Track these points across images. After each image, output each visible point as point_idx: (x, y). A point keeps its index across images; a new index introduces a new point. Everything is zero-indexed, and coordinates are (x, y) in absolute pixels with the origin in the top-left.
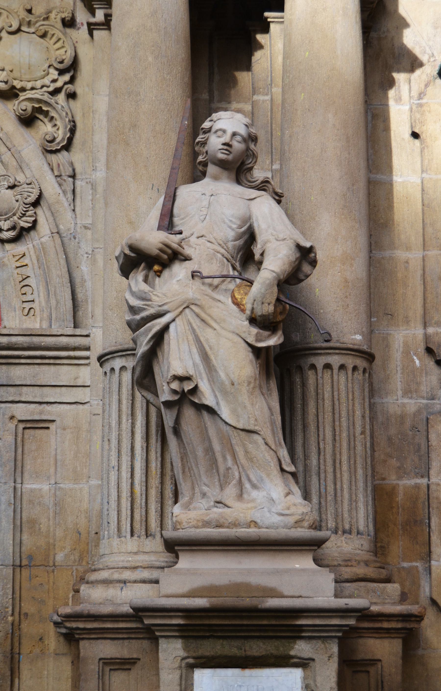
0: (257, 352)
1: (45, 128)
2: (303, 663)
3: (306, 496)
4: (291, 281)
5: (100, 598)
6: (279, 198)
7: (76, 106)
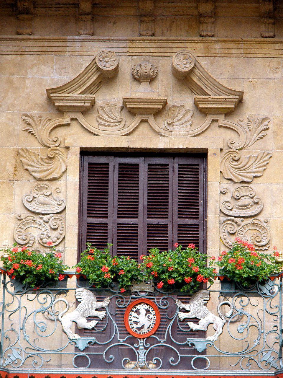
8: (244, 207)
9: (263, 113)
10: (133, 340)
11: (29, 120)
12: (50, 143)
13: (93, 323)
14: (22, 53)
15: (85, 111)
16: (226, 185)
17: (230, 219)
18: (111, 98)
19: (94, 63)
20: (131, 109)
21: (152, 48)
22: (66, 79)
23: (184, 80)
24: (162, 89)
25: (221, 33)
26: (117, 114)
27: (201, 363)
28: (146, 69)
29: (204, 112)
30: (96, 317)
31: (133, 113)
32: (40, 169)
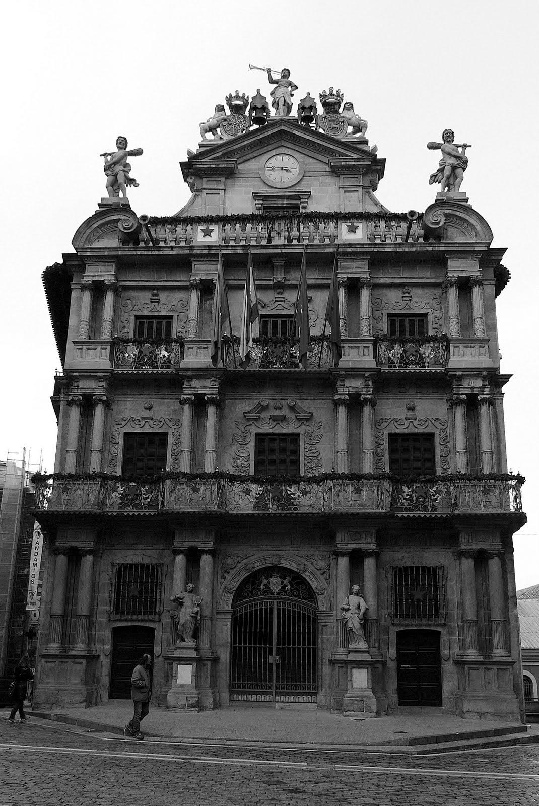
0: (360, 624)
2: (367, 668)
3: (368, 644)
4: (364, 613)
5: (338, 657)
6: (363, 598)
7: (330, 571)
8: (313, 453)
11: (237, 423)
12: (246, 432)
14: (235, 399)
15: (256, 420)
16: (307, 445)
17: (308, 458)
18: (265, 415)
19: (260, 403)
20: (274, 419)
21: (280, 397)
22: (250, 408)
23: (292, 408)
24: (285, 412)
27: (296, 509)
28: (278, 404)
29: (299, 420)
30: (259, 494)
31: (273, 420)
32: (241, 440)
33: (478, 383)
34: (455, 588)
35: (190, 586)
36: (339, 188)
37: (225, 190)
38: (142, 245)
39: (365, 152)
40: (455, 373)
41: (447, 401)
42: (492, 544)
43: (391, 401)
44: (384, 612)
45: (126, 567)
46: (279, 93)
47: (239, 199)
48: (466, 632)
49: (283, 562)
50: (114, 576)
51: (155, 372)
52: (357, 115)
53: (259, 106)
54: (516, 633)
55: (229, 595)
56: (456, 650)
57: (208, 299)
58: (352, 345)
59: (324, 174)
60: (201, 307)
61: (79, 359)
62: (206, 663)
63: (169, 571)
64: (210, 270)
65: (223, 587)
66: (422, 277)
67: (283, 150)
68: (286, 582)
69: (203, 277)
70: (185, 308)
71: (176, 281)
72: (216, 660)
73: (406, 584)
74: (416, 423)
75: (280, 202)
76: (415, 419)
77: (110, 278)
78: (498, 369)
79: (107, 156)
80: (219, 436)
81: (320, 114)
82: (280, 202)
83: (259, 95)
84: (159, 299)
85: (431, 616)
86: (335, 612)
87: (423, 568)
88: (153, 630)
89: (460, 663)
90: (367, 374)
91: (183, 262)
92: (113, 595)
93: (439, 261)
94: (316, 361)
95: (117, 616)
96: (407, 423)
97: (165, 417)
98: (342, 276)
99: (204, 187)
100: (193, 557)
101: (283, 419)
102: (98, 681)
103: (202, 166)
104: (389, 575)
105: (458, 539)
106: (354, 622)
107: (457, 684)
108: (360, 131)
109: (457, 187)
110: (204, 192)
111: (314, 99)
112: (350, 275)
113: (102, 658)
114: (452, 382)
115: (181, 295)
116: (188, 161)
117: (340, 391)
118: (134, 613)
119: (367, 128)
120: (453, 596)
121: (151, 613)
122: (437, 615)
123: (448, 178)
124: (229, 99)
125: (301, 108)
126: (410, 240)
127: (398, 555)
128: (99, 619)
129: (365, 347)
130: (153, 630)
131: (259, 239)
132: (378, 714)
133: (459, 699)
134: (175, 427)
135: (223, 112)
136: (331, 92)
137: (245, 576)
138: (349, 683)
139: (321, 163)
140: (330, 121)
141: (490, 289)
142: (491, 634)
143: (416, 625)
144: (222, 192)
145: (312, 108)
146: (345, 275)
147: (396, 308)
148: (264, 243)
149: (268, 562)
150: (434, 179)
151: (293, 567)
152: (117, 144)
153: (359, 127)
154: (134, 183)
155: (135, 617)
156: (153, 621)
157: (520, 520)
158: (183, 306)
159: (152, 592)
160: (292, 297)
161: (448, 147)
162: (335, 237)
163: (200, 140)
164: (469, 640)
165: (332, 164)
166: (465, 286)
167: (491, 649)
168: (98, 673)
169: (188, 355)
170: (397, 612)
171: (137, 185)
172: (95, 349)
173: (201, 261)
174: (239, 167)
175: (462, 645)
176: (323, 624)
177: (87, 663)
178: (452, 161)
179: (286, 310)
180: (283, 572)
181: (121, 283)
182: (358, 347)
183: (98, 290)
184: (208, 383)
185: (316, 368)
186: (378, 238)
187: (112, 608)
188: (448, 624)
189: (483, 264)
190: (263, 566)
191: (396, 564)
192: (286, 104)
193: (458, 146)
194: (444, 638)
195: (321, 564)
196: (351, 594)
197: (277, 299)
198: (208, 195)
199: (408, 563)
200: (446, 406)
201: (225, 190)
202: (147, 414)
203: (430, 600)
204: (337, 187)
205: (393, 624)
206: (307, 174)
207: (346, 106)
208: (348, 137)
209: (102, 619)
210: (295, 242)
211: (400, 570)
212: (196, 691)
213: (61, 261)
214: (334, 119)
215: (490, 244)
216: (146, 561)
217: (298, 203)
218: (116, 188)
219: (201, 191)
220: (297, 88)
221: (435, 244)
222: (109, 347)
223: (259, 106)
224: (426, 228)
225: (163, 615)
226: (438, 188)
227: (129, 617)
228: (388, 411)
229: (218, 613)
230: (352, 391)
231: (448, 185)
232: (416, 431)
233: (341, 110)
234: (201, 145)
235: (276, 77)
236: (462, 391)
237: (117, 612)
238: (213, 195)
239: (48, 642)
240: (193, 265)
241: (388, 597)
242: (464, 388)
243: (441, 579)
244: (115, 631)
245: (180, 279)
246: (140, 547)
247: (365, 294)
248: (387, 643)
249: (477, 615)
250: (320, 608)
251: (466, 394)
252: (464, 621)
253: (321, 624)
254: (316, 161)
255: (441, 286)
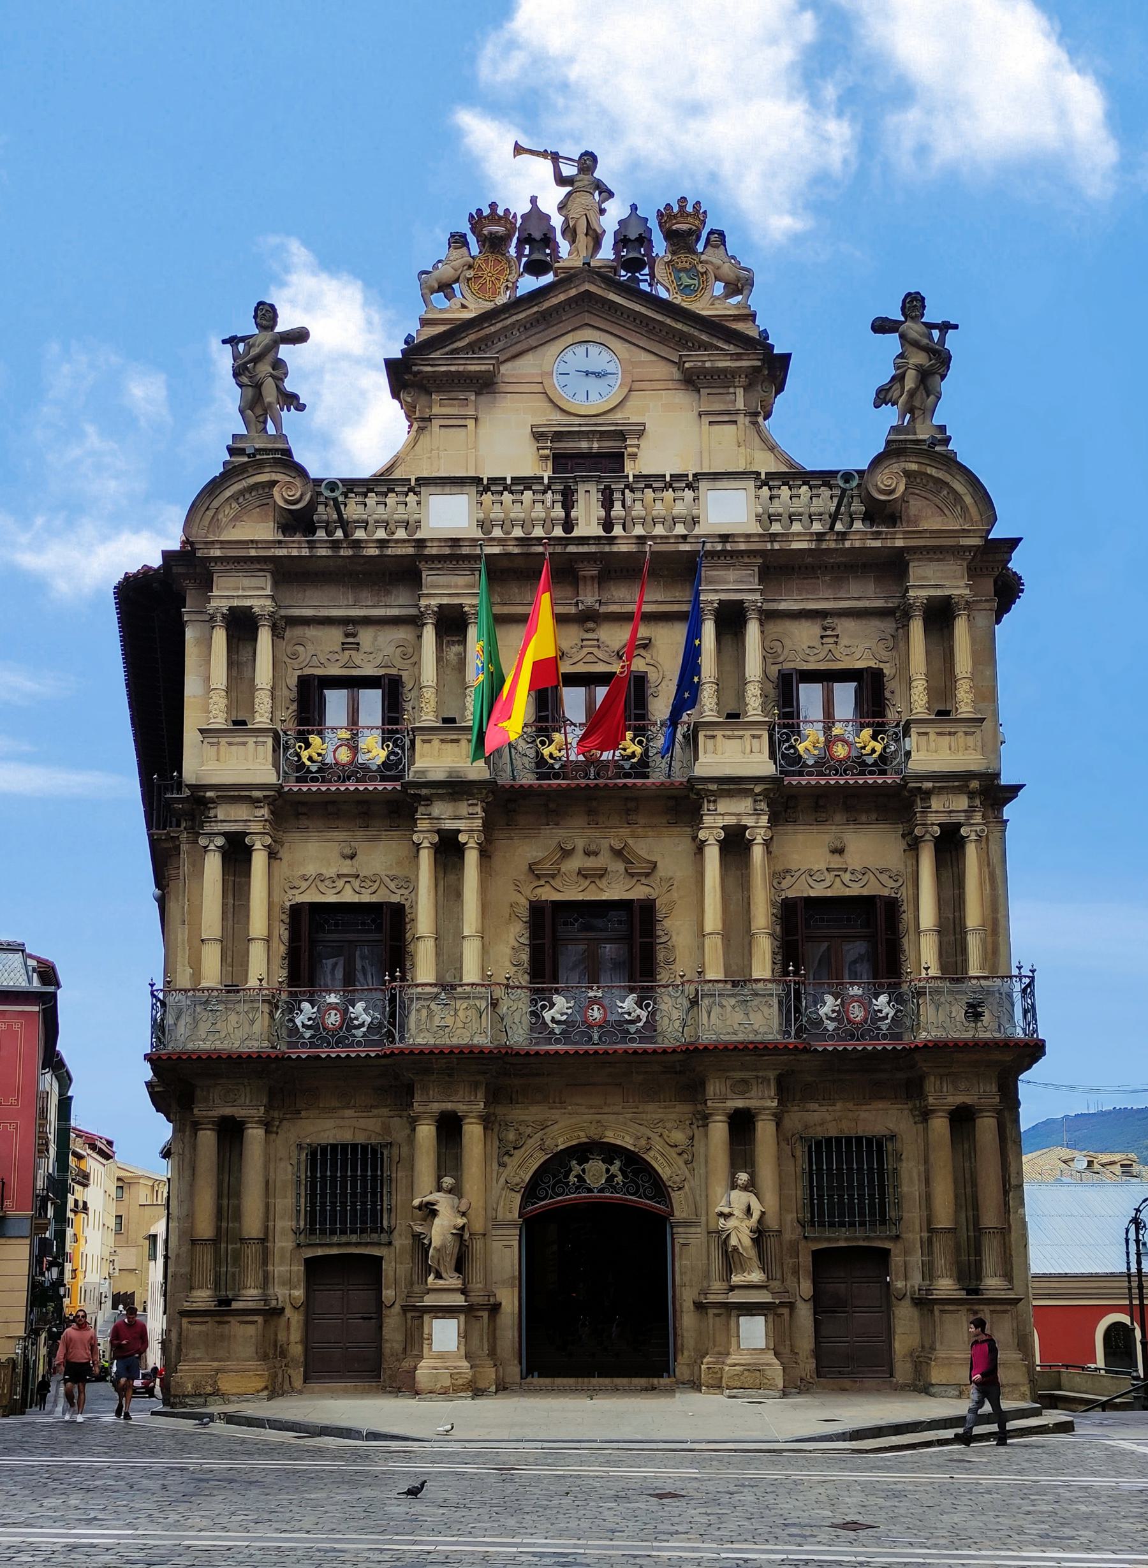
1: (685, 1156)
9: (670, 874)
10: (590, 1026)
13: (565, 1017)
14: (511, 838)
15: (553, 876)
20: (582, 874)
22: (541, 855)
23: (618, 854)
24: (604, 860)
25: (642, 821)
26: (575, 878)
28: (593, 847)
29: (632, 875)
31: (585, 877)
33: (962, 802)
34: (915, 1175)
35: (448, 1181)
36: (700, 415)
37: (476, 419)
38: (321, 534)
39: (747, 342)
40: (919, 785)
41: (903, 836)
42: (979, 1093)
43: (800, 837)
44: (790, 1217)
45: (324, 1149)
46: (576, 209)
47: (504, 439)
48: (936, 1249)
49: (609, 1133)
50: (303, 1168)
51: (361, 788)
52: (733, 257)
53: (537, 235)
54: (1021, 1249)
55: (514, 1194)
56: (916, 1280)
57: (454, 643)
58: (729, 733)
59: (670, 385)
60: (439, 660)
61: (212, 765)
62: (480, 1313)
63: (403, 1155)
64: (456, 587)
65: (502, 1180)
66: (859, 599)
67: (588, 334)
68: (615, 1168)
69: (445, 601)
70: (408, 661)
71: (386, 606)
72: (495, 1309)
73: (830, 1169)
74: (846, 877)
75: (584, 445)
76: (846, 870)
77: (262, 602)
78: (997, 775)
79: (237, 344)
80: (485, 908)
81: (662, 254)
82: (584, 445)
83: (536, 214)
84: (358, 644)
85: (873, 1223)
86: (703, 1219)
87: (859, 1139)
88: (381, 1258)
89: (924, 1303)
90: (758, 789)
91: (403, 570)
92: (303, 1200)
93: (892, 567)
94: (662, 766)
95: (313, 1237)
96: (829, 877)
97: (383, 873)
98: (710, 598)
99: (436, 410)
100: (450, 1129)
101: (602, 874)
102: (283, 1354)
103: (429, 369)
104: (798, 1153)
105: (921, 1087)
106: (741, 1235)
107: (918, 1340)
108: (738, 291)
109: (928, 414)
110: (436, 423)
111: (646, 220)
112: (724, 597)
113: (289, 1312)
114: (914, 801)
115: (402, 634)
116: (400, 356)
117: (708, 820)
118: (343, 1232)
119: (752, 286)
120: (910, 1186)
121: (374, 1230)
122: (883, 1222)
123: (912, 394)
124: (477, 221)
125: (621, 240)
126: (839, 527)
127: (816, 1117)
128: (278, 1244)
129: (753, 736)
130: (381, 1258)
131: (548, 522)
132: (785, 1394)
133: (921, 1361)
134: (402, 891)
135: (464, 249)
136: (682, 208)
137: (542, 1160)
138: (734, 1340)
139: (663, 363)
140: (680, 270)
141: (983, 619)
142: (978, 1252)
143: (846, 1239)
144: (471, 423)
145: (644, 240)
146: (714, 597)
147: (811, 659)
148: (558, 532)
149: (582, 1134)
150: (882, 397)
151: (628, 1142)
152: (255, 317)
153: (739, 285)
154: (295, 403)
155: (344, 1239)
156: (379, 1244)
157: (1032, 1051)
158: (404, 656)
159: (374, 1194)
160: (616, 636)
161: (913, 329)
162: (695, 521)
163: (421, 311)
164: (941, 1262)
165: (687, 365)
166: (940, 616)
167: (979, 1277)
168: (282, 1336)
169: (422, 756)
170: (813, 1216)
171: (301, 408)
172: (244, 744)
173: (439, 569)
174: (503, 369)
175: (929, 1272)
176: (681, 1241)
177: (265, 1321)
178: (919, 358)
179: (601, 663)
180: (610, 1152)
181: (283, 612)
182: (741, 737)
183: (241, 626)
184: (464, 808)
185: (662, 779)
186: (776, 520)
187: (302, 1223)
188: (904, 1236)
189: (973, 572)
190: (574, 1143)
191: (811, 1133)
192: (591, 232)
193: (930, 326)
194: (897, 1260)
195: (679, 1137)
196: (734, 1186)
197: (585, 643)
198: (443, 429)
199: (833, 1133)
200: (902, 845)
201: (476, 419)
202: (346, 867)
203: (872, 1196)
204: (695, 413)
205: (805, 1238)
206: (636, 385)
207: (713, 238)
208: (717, 306)
209: (283, 1243)
210: (618, 531)
211: (818, 1144)
212: (467, 1364)
213: (156, 562)
214: (687, 265)
215: (989, 531)
216: (361, 1139)
217: (621, 447)
218: (259, 411)
219: (430, 419)
220: (611, 195)
221: (887, 533)
222: (270, 742)
223: (537, 235)
224: (869, 500)
225: (396, 1233)
226: (890, 415)
227: (335, 1239)
228: (795, 856)
229: (496, 1227)
230: (732, 821)
231: (911, 410)
232: (848, 892)
233: (700, 247)
234: (424, 322)
235: (568, 170)
236: (932, 818)
237: (312, 1231)
238: (454, 429)
239: (192, 1288)
240: (424, 576)
241: (797, 1192)
242: (937, 812)
243: (890, 1158)
244: (310, 1263)
245: (396, 605)
246: (349, 1113)
247: (753, 630)
248: (796, 1272)
249: (957, 1222)
250: (679, 1214)
251: (939, 825)
252: (931, 1230)
253: (679, 1241)
254: (654, 358)
255: (900, 615)
